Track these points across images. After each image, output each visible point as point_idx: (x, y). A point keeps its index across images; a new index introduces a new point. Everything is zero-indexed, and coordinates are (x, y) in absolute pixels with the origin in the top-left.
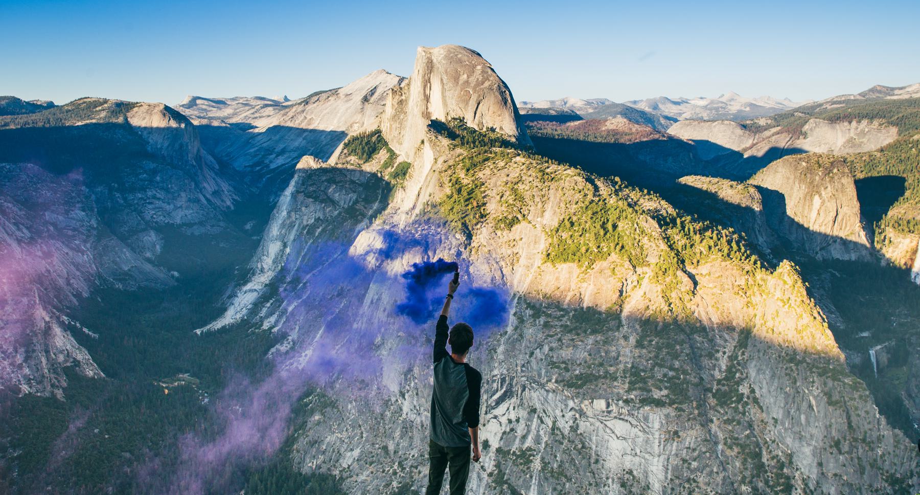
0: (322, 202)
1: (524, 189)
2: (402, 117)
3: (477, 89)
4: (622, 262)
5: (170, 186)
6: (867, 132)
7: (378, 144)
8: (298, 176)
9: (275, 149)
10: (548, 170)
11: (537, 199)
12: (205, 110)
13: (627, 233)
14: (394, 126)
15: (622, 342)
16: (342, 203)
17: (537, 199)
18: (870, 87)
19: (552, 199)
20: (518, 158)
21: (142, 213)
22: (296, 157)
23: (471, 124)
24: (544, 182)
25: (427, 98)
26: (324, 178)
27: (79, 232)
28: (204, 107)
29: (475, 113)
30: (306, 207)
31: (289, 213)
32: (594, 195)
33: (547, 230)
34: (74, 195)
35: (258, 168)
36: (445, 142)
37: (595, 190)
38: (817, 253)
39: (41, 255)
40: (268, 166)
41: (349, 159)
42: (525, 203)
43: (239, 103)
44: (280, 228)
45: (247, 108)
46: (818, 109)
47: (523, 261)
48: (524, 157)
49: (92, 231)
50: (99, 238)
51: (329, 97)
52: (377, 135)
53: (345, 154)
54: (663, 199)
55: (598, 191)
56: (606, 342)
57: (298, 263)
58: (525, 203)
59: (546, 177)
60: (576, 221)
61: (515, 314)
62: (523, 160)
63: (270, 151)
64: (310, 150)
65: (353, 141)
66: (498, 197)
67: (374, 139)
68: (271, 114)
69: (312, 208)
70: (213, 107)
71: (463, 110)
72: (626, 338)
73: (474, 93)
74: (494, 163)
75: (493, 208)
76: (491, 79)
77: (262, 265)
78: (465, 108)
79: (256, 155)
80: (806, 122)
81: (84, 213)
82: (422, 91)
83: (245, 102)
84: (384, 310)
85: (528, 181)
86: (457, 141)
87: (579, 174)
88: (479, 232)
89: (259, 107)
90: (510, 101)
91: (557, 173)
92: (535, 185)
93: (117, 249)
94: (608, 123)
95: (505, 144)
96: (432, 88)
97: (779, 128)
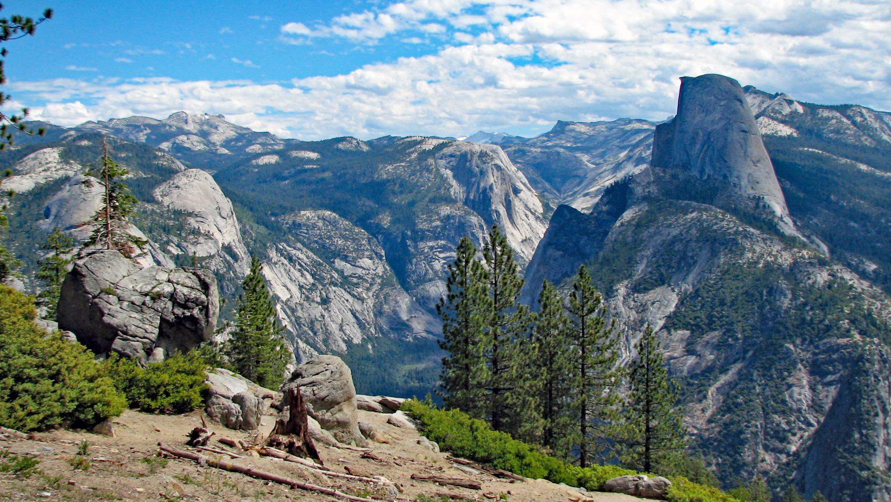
15: (698, 413)
20: (694, 214)
21: (431, 262)
27: (364, 279)
31: (539, 265)
34: (364, 242)
39: (318, 300)
49: (376, 279)
50: (383, 285)
56: (683, 412)
72: (703, 410)
73: (704, 135)
75: (640, 269)
79: (596, 196)
81: (370, 261)
88: (616, 293)
93: (398, 298)
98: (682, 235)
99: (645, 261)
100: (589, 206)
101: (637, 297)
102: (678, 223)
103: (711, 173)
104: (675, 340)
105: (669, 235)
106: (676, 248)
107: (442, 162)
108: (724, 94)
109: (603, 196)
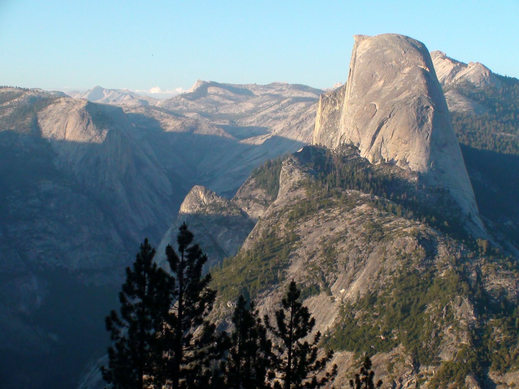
2: (331, 136)
3: (387, 103)
5: (67, 216)
10: (388, 225)
11: (351, 264)
12: (218, 104)
13: (431, 316)
17: (351, 264)
19: (369, 265)
20: (363, 207)
24: (370, 241)
28: (216, 98)
29: (374, 138)
41: (254, 193)
42: (334, 268)
43: (265, 94)
53: (251, 185)
55: (433, 258)
58: (334, 268)
60: (380, 297)
70: (230, 98)
71: (360, 133)
73: (379, 109)
76: (414, 88)
83: (275, 93)
89: (285, 101)
99: (300, 262)
102: (343, 217)
106: (339, 247)
107: (48, 122)
108: (407, 58)
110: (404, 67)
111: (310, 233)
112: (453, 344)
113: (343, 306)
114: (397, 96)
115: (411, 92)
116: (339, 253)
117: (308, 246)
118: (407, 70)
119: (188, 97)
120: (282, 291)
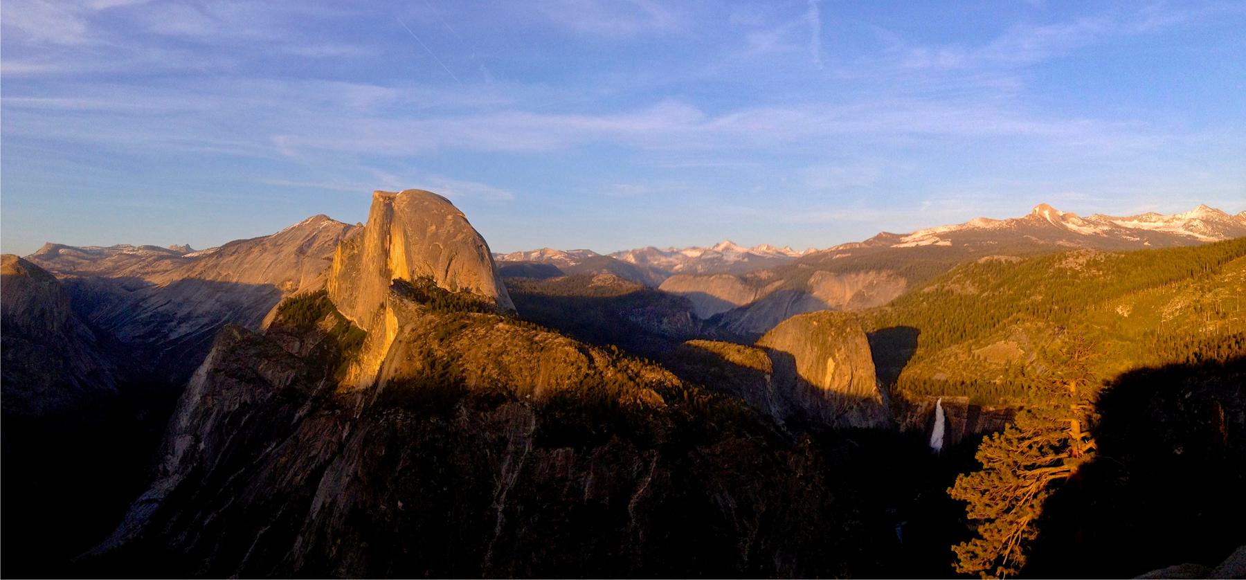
0: (249, 382)
1: (509, 361)
2: (354, 275)
4: (625, 445)
6: (876, 284)
7: (323, 308)
8: (217, 350)
9: (176, 313)
10: (537, 338)
14: (344, 286)
16: (276, 383)
18: (876, 235)
20: (501, 325)
22: (207, 324)
23: (440, 284)
24: (533, 353)
25: (386, 253)
26: (252, 352)
29: (447, 272)
30: (228, 389)
31: (204, 398)
32: (589, 368)
33: (538, 409)
35: (152, 340)
36: (412, 306)
37: (590, 361)
38: (833, 422)
40: (166, 336)
42: (511, 377)
43: (121, 254)
44: (190, 418)
45: (134, 260)
46: (823, 259)
47: (511, 448)
48: (508, 323)
51: (251, 248)
52: (322, 297)
54: (666, 369)
55: (593, 363)
57: (217, 461)
59: (535, 346)
61: (503, 512)
62: (507, 327)
63: (169, 316)
64: (226, 314)
65: (291, 305)
66: (479, 372)
67: (318, 302)
68: (168, 268)
69: (236, 391)
70: (83, 258)
74: (473, 331)
77: (165, 467)
78: (434, 265)
80: (811, 275)
82: (379, 244)
84: (340, 517)
85: (513, 351)
86: (427, 305)
87: (570, 344)
89: (151, 259)
90: (487, 257)
91: (547, 342)
92: (522, 356)
94: (595, 280)
95: (481, 307)
96: (392, 241)
97: (783, 281)
98: (506, 347)
100: (142, 334)
101: (485, 416)
103: (464, 286)
104: (559, 459)
105: (490, 345)
109: (277, 316)
110: (446, 215)
111: (469, 350)
112: (660, 429)
113: (535, 410)
114: (455, 238)
115: (464, 235)
116: (509, 364)
117: (474, 361)
118: (450, 217)
119: (42, 257)
120: (472, 402)
